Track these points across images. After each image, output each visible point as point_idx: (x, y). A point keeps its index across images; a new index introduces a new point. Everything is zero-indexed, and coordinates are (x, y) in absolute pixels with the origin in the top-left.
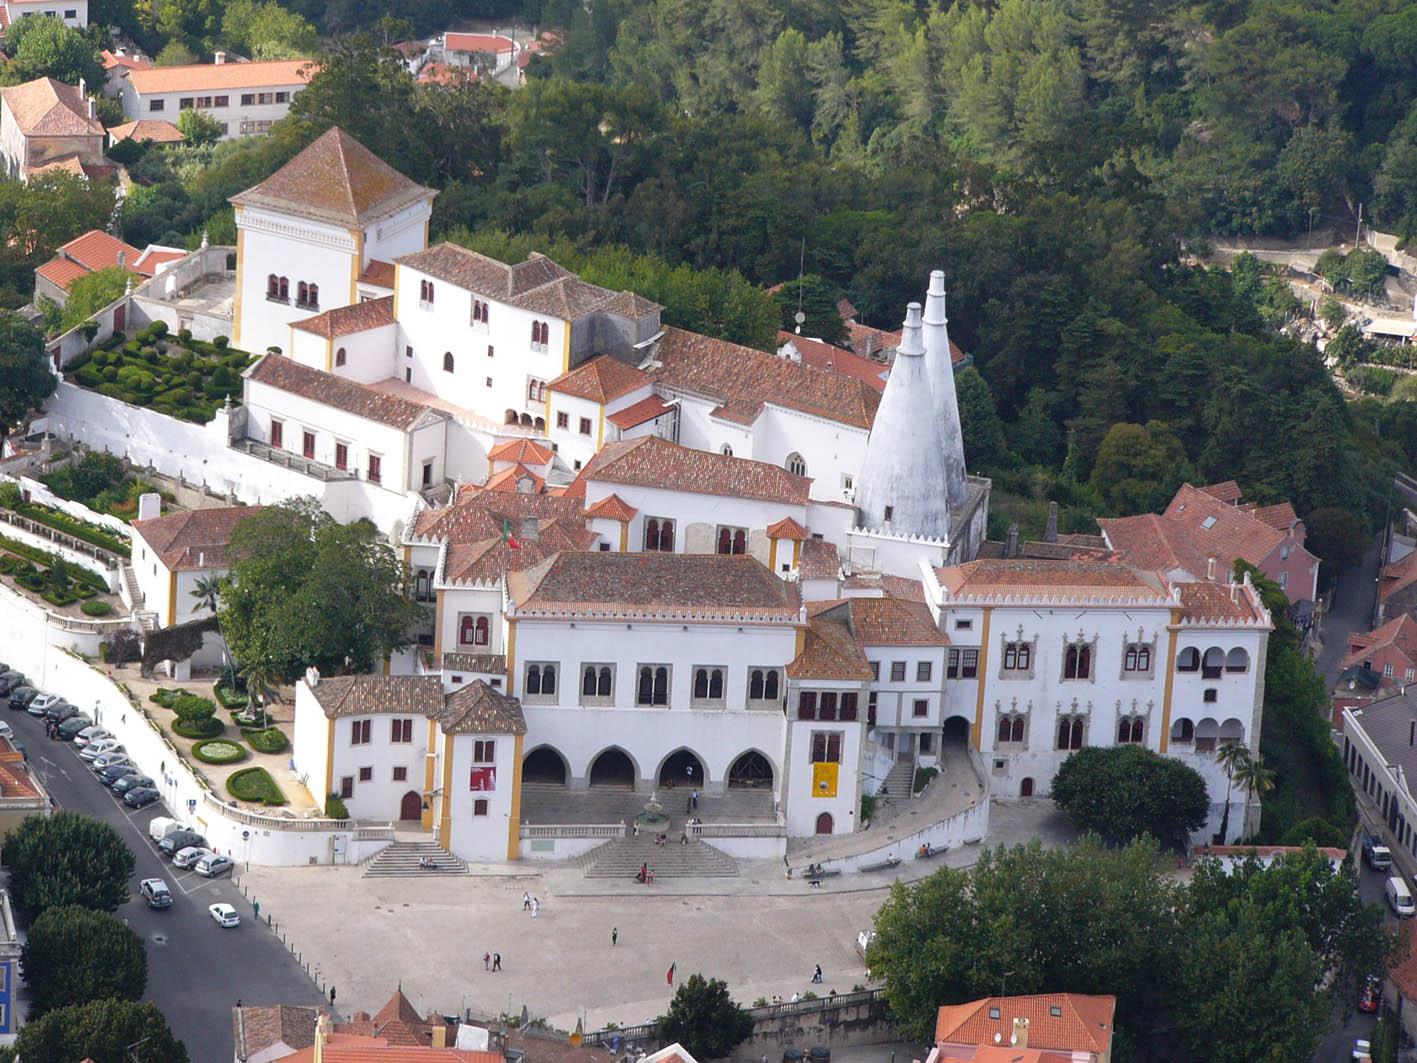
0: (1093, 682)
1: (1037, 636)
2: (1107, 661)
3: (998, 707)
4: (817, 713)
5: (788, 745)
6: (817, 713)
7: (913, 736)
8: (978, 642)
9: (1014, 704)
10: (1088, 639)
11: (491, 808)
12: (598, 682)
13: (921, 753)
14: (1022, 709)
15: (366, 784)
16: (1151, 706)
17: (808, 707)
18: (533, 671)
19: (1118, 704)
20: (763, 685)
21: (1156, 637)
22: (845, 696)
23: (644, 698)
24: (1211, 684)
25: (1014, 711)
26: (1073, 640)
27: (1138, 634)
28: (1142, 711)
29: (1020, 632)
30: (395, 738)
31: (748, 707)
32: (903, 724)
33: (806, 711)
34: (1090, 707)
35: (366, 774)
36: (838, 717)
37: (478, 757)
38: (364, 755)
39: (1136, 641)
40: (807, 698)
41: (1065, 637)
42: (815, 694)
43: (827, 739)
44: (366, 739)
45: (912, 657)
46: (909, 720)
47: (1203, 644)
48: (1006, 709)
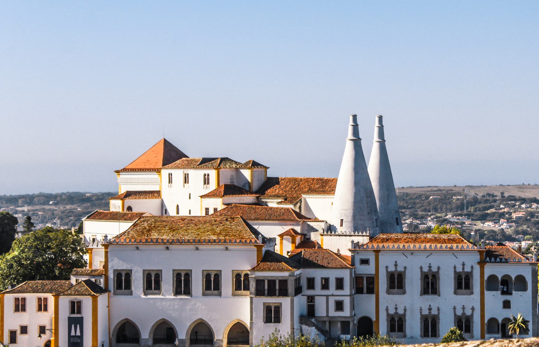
0: (439, 296)
1: (405, 268)
2: (447, 283)
3: (387, 310)
4: (266, 292)
6: (266, 292)
8: (373, 272)
9: (396, 309)
10: (434, 269)
13: (342, 334)
14: (401, 311)
15: (25, 337)
16: (473, 309)
18: (118, 274)
19: (455, 308)
21: (472, 267)
24: (507, 297)
25: (396, 313)
26: (426, 269)
27: (462, 267)
28: (468, 312)
29: (396, 265)
32: (330, 315)
33: (259, 292)
34: (439, 309)
37: (73, 312)
38: (23, 319)
39: (461, 270)
40: (259, 282)
41: (421, 268)
44: (24, 309)
48: (392, 311)
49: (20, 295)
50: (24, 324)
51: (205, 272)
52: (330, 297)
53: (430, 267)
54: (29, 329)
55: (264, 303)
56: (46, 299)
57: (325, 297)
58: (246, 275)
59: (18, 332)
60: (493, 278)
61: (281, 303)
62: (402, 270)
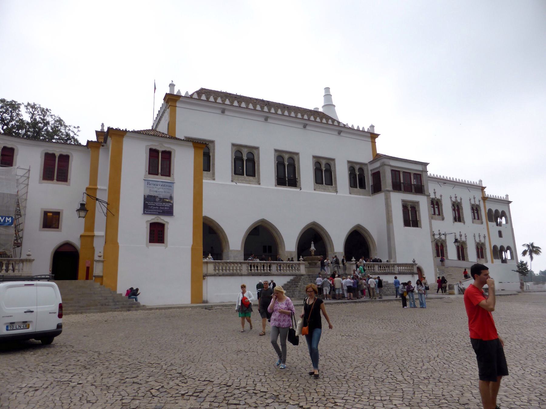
1: (441, 196)
11: (170, 233)
12: (245, 164)
16: (485, 237)
19: (474, 236)
21: (479, 201)
23: (281, 181)
24: (499, 228)
26: (454, 200)
29: (435, 193)
33: (397, 187)
34: (466, 236)
36: (413, 191)
37: (152, 170)
41: (451, 198)
43: (410, 209)
47: (494, 207)
53: (456, 197)
55: (403, 201)
60: (490, 210)
61: (418, 203)
62: (439, 198)
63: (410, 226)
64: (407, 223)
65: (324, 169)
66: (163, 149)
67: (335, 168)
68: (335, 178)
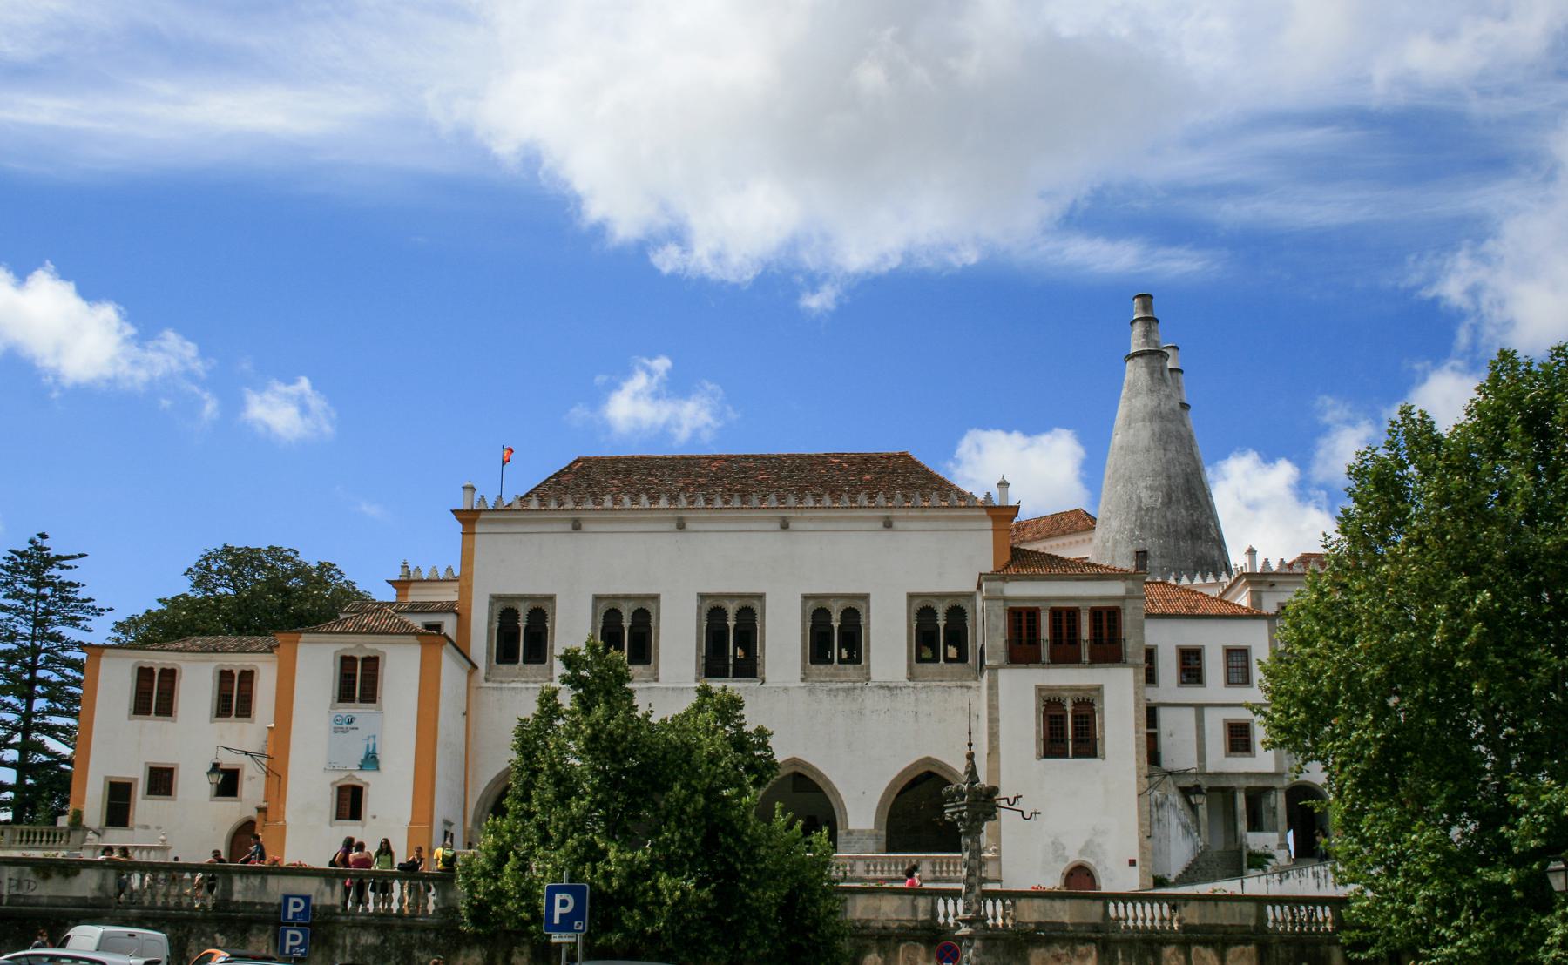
5: (993, 721)
7: (1228, 794)
17: (1027, 639)
18: (505, 613)
20: (939, 633)
22: (1096, 614)
30: (224, 708)
31: (912, 676)
32: (1209, 769)
35: (161, 781)
40: (1022, 621)
42: (1033, 614)
43: (1069, 708)
44: (166, 708)
45: (1213, 640)
46: (1219, 760)
49: (157, 660)
50: (162, 760)
51: (811, 603)
52: (1208, 712)
54: (181, 782)
56: (248, 677)
57: (1190, 713)
58: (957, 615)
59: (140, 789)
63: (1066, 756)
64: (1053, 745)
65: (836, 625)
66: (364, 655)
67: (868, 617)
68: (868, 644)
